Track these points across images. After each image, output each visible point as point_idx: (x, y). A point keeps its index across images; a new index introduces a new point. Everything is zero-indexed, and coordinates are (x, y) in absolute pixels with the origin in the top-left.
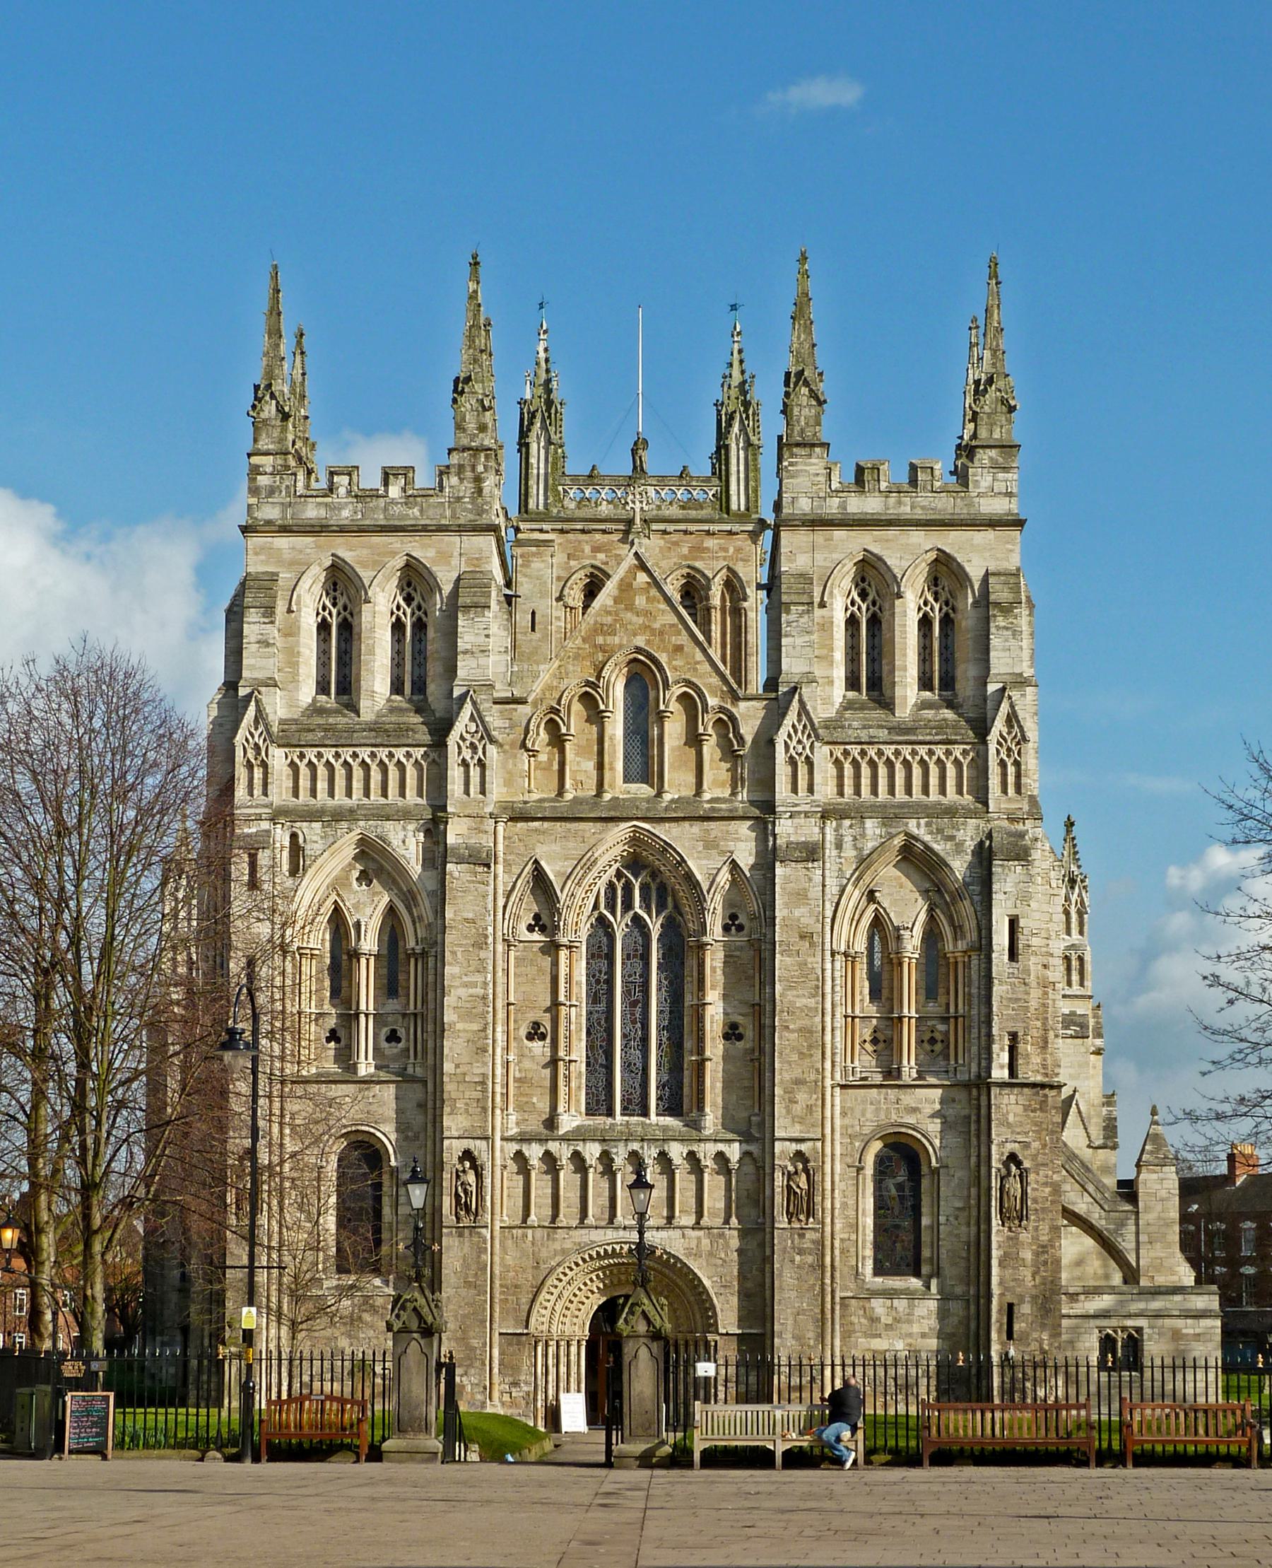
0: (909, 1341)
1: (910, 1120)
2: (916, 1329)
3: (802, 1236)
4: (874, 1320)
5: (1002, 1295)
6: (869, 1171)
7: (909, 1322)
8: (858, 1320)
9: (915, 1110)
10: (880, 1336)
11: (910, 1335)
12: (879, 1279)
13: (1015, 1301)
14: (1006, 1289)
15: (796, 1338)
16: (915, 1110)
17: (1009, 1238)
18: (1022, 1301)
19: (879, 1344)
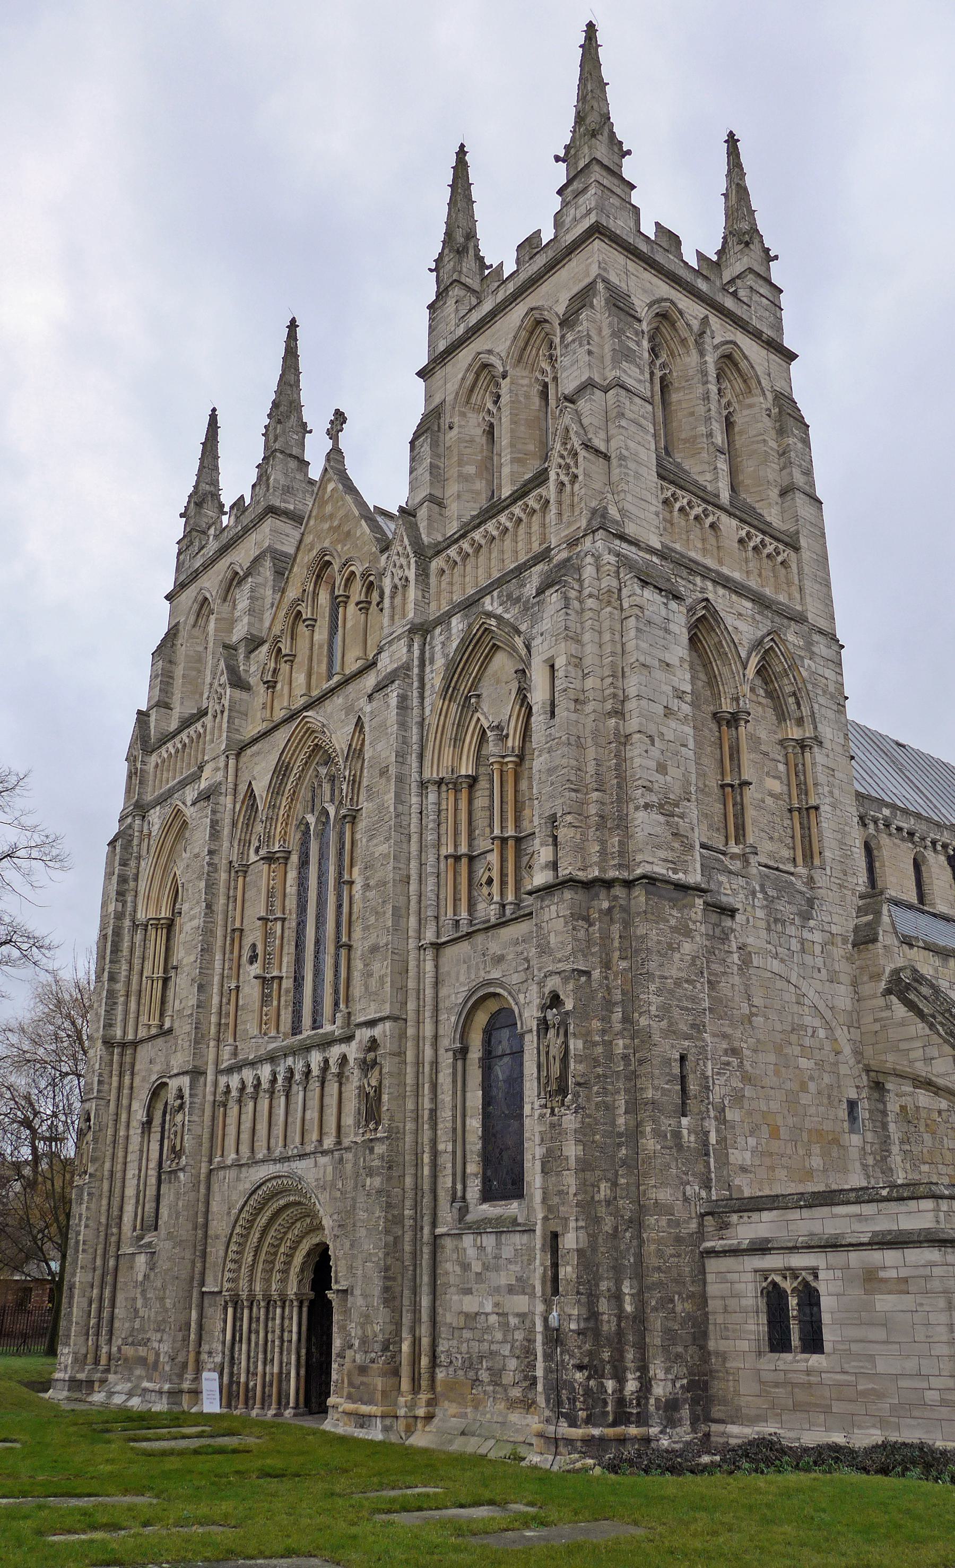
0: (497, 1298)
1: (495, 974)
2: (503, 1279)
3: (372, 1150)
4: (466, 1267)
5: (545, 1219)
6: (475, 1054)
7: (497, 1269)
8: (449, 1267)
9: (499, 959)
10: (469, 1291)
11: (497, 1290)
12: (485, 1206)
13: (559, 1229)
14: (550, 1209)
15: (365, 1296)
16: (499, 959)
17: (553, 1126)
18: (566, 1226)
19: (470, 1304)
